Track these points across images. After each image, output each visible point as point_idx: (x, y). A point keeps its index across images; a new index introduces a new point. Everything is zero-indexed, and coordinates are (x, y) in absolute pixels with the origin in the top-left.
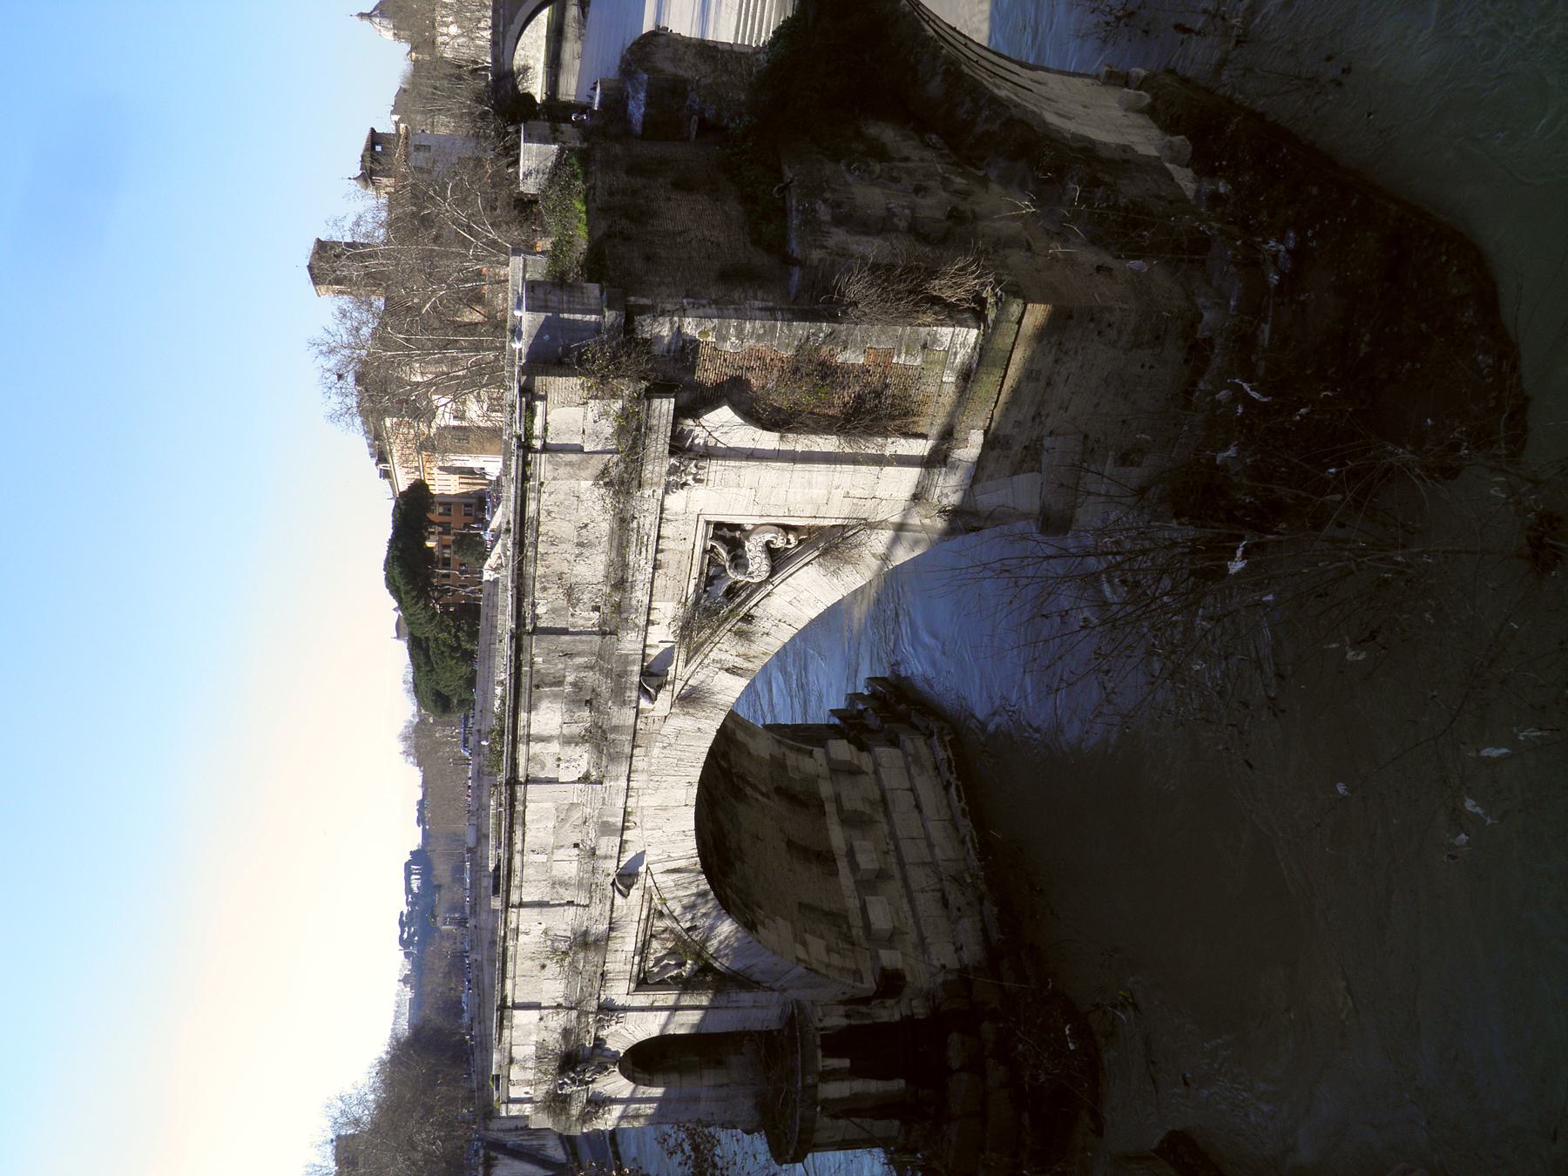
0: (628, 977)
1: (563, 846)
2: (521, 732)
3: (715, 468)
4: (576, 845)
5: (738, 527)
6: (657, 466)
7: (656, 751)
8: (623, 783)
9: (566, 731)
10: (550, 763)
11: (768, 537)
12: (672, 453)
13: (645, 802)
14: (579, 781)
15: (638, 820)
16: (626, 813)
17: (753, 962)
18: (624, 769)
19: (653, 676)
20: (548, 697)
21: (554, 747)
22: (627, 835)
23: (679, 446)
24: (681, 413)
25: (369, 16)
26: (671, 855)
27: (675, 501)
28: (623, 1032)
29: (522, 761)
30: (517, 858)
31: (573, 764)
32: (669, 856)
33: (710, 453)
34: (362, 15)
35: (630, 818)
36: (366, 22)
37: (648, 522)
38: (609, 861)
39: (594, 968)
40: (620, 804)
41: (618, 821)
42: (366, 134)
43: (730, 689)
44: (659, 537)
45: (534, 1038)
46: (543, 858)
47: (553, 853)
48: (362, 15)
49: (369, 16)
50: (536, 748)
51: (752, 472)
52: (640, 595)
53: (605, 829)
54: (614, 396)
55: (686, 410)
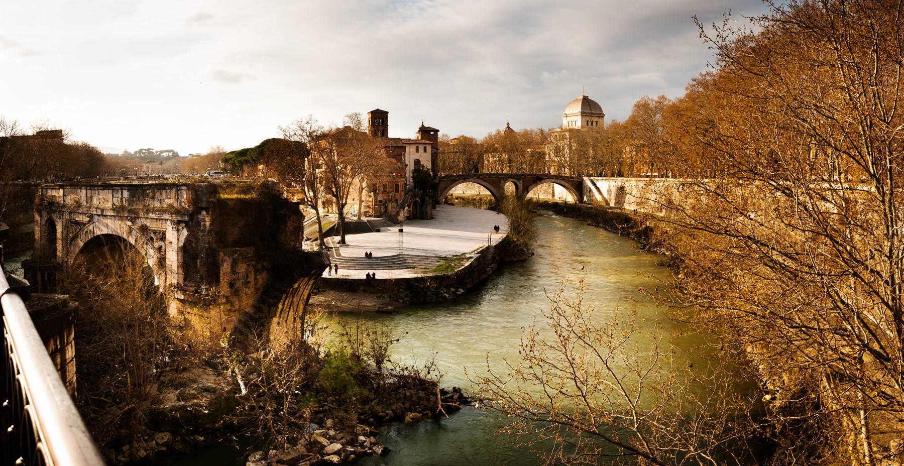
3: (175, 233)
5: (165, 240)
6: (176, 218)
7: (120, 222)
8: (112, 214)
9: (124, 199)
10: (117, 195)
11: (163, 248)
12: (178, 221)
13: (109, 221)
14: (113, 203)
16: (106, 216)
18: (115, 214)
19: (133, 220)
21: (120, 196)
22: (101, 217)
23: (179, 222)
24: (186, 222)
25: (508, 127)
27: (169, 223)
29: (117, 188)
30: (96, 188)
33: (178, 231)
34: (508, 124)
36: (506, 126)
37: (166, 216)
40: (108, 214)
41: (104, 214)
42: (437, 129)
43: (132, 240)
44: (162, 219)
45: (57, 195)
48: (508, 124)
49: (508, 127)
50: (120, 192)
51: (175, 241)
52: (151, 215)
53: (103, 210)
54: (189, 206)
55: (186, 222)
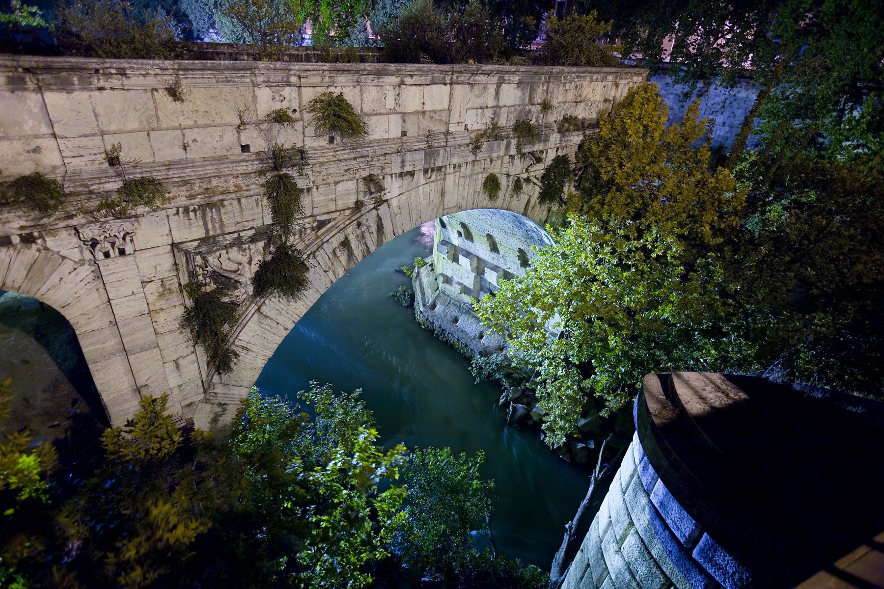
0: (211, 233)
1: (404, 121)
2: (506, 77)
4: (404, 134)
15: (433, 178)
17: (254, 348)
20: (524, 94)
21: (491, 102)
22: (420, 178)
26: (398, 218)
28: (68, 265)
31: (479, 119)
32: (396, 215)
35: (435, 172)
38: (400, 165)
39: (232, 188)
46: (390, 103)
47: (398, 113)
